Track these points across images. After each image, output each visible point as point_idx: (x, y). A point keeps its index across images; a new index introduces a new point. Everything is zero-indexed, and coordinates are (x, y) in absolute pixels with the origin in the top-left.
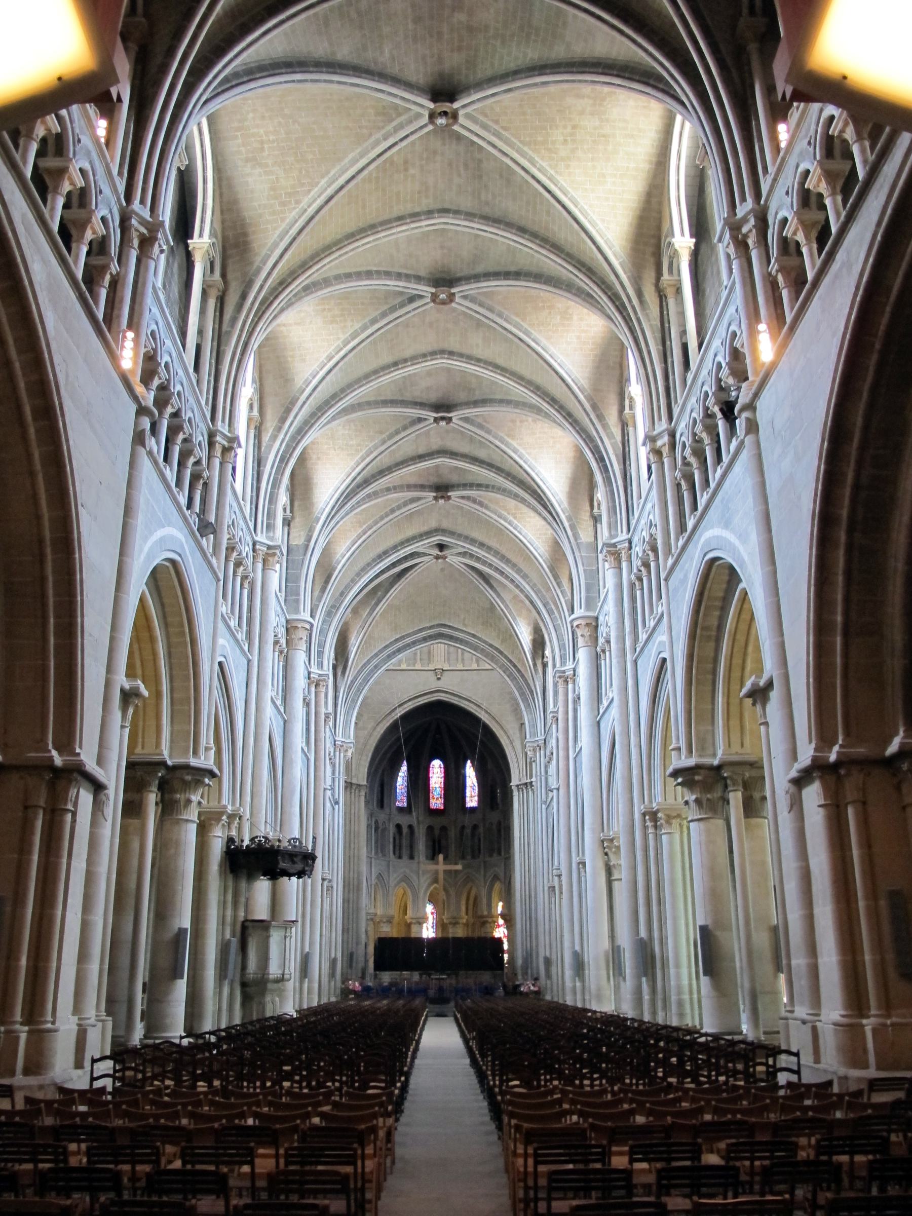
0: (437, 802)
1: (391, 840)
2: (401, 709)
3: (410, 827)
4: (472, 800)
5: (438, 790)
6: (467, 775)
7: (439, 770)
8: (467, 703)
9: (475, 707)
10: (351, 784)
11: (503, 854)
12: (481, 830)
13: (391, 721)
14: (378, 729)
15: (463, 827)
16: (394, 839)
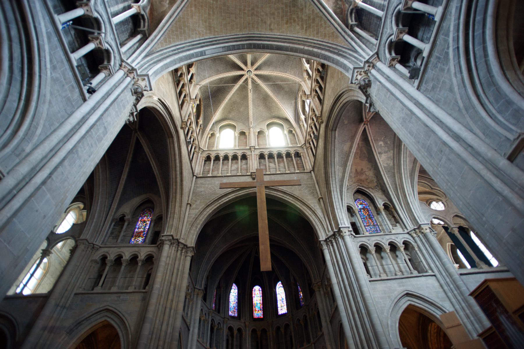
0: (258, 313)
1: (225, 338)
2: (226, 198)
3: (239, 330)
4: (282, 308)
5: (259, 305)
6: (277, 293)
7: (258, 292)
8: (275, 192)
9: (282, 194)
10: (179, 243)
11: (312, 340)
12: (292, 327)
13: (218, 205)
14: (208, 210)
15: (278, 328)
16: (227, 340)
